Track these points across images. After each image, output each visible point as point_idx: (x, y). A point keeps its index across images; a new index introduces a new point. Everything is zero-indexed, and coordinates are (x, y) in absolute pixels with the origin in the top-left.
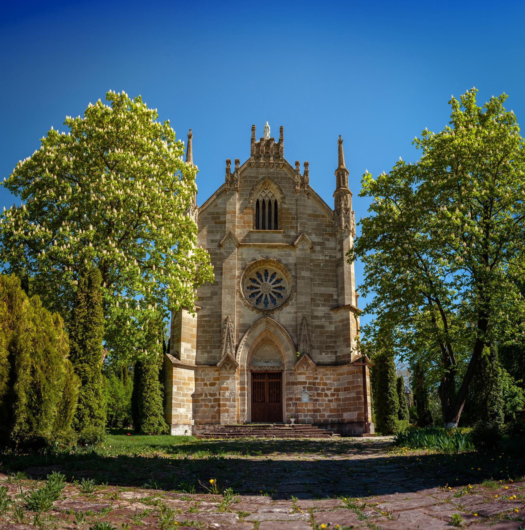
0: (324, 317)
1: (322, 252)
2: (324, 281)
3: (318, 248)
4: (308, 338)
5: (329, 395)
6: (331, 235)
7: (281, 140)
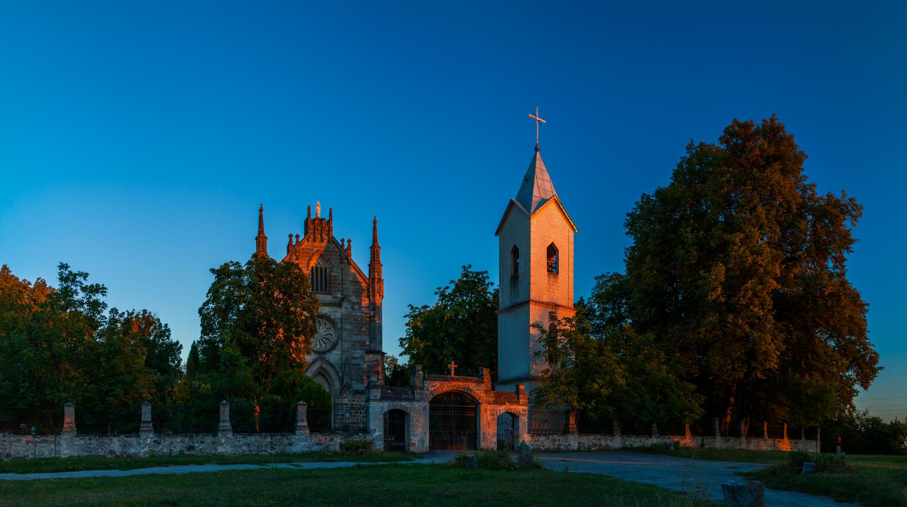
3: (356, 307)
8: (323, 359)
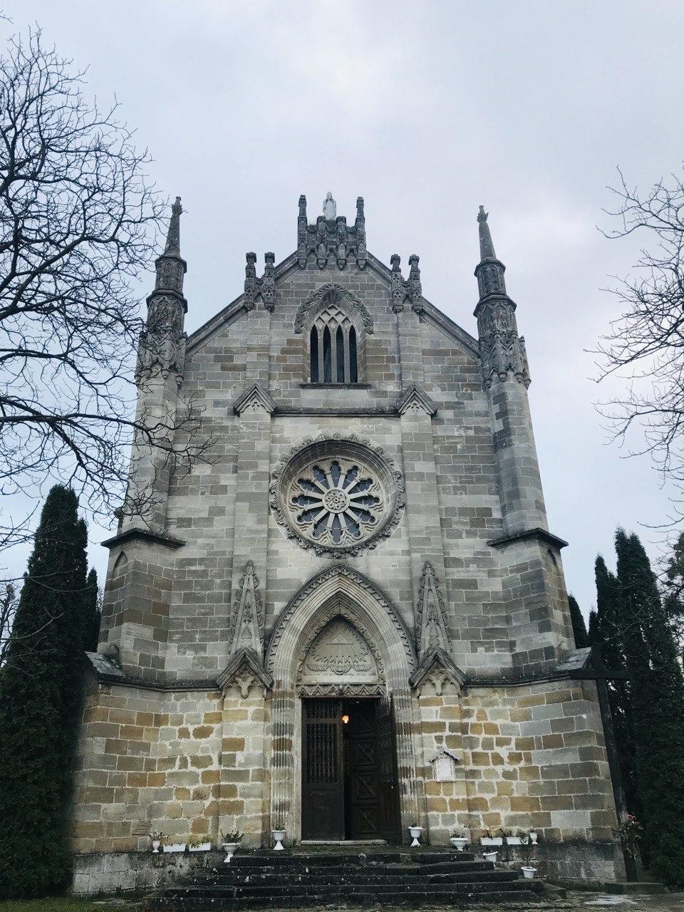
0: (474, 560)
1: (457, 421)
2: (465, 482)
4: (439, 612)
5: (506, 760)
6: (474, 387)
7: (360, 219)
8: (341, 570)
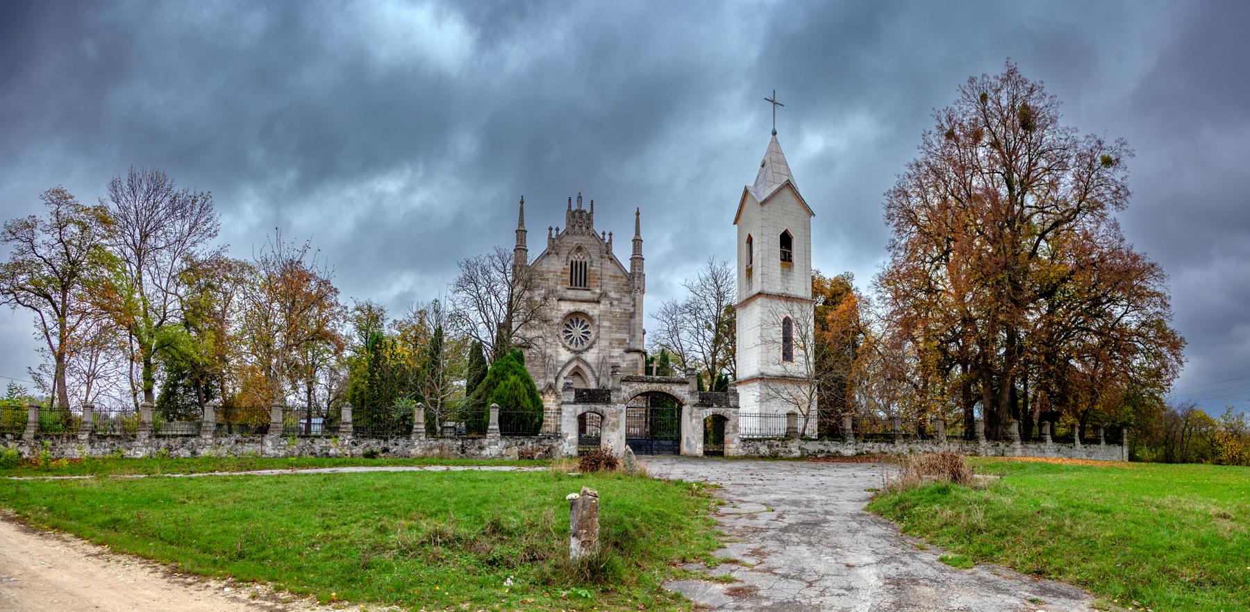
8: (578, 359)
